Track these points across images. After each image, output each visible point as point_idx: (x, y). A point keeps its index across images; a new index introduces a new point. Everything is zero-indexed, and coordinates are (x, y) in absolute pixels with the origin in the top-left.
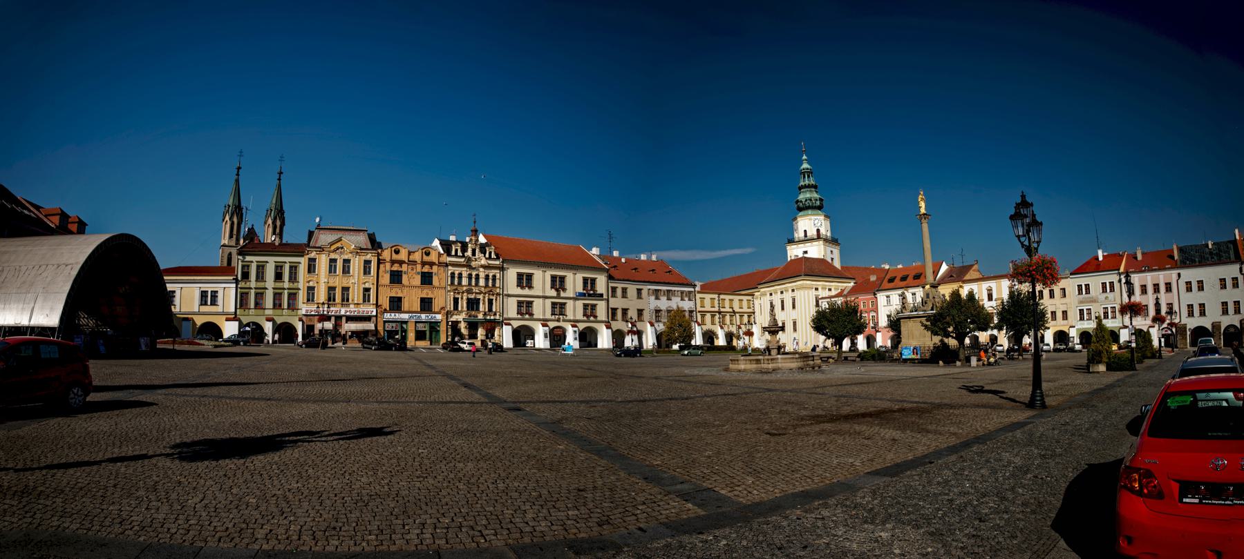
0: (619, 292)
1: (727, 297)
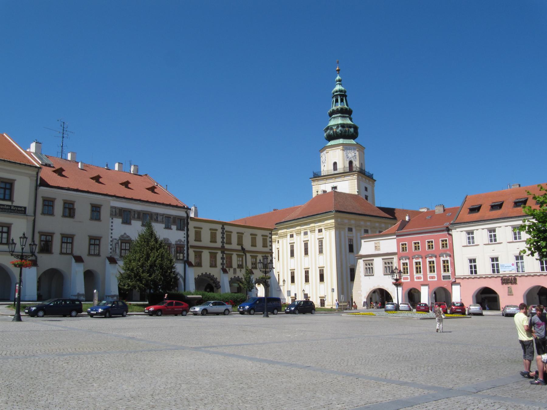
0: (59, 208)
1: (235, 230)
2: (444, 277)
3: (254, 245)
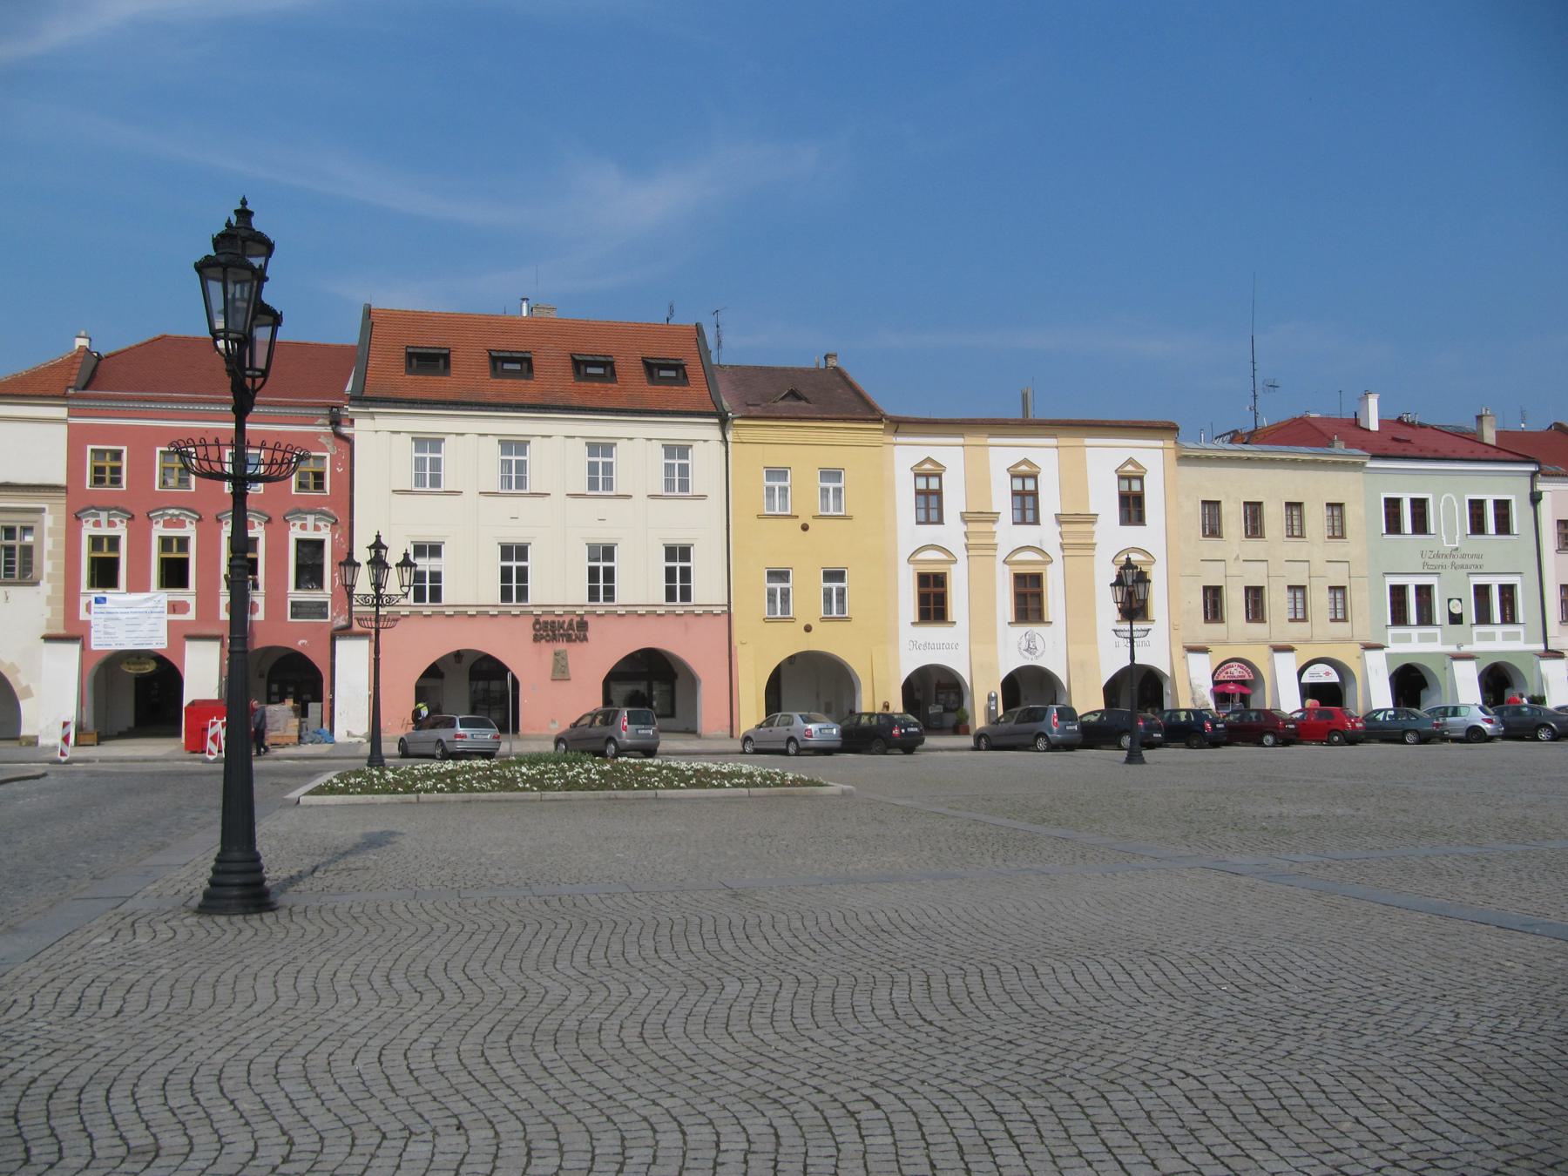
2: (299, 609)
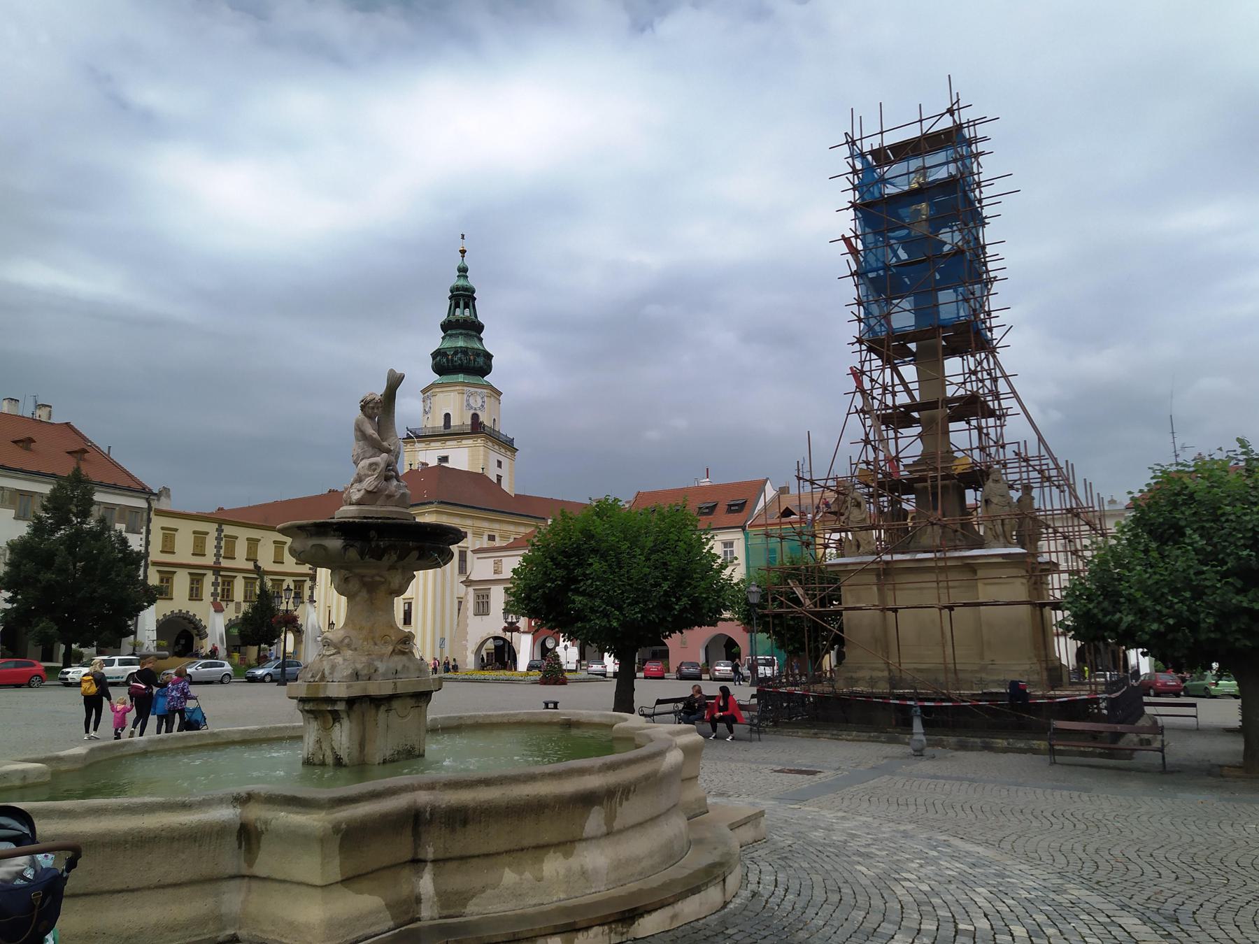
1: (243, 534)
3: (278, 561)
